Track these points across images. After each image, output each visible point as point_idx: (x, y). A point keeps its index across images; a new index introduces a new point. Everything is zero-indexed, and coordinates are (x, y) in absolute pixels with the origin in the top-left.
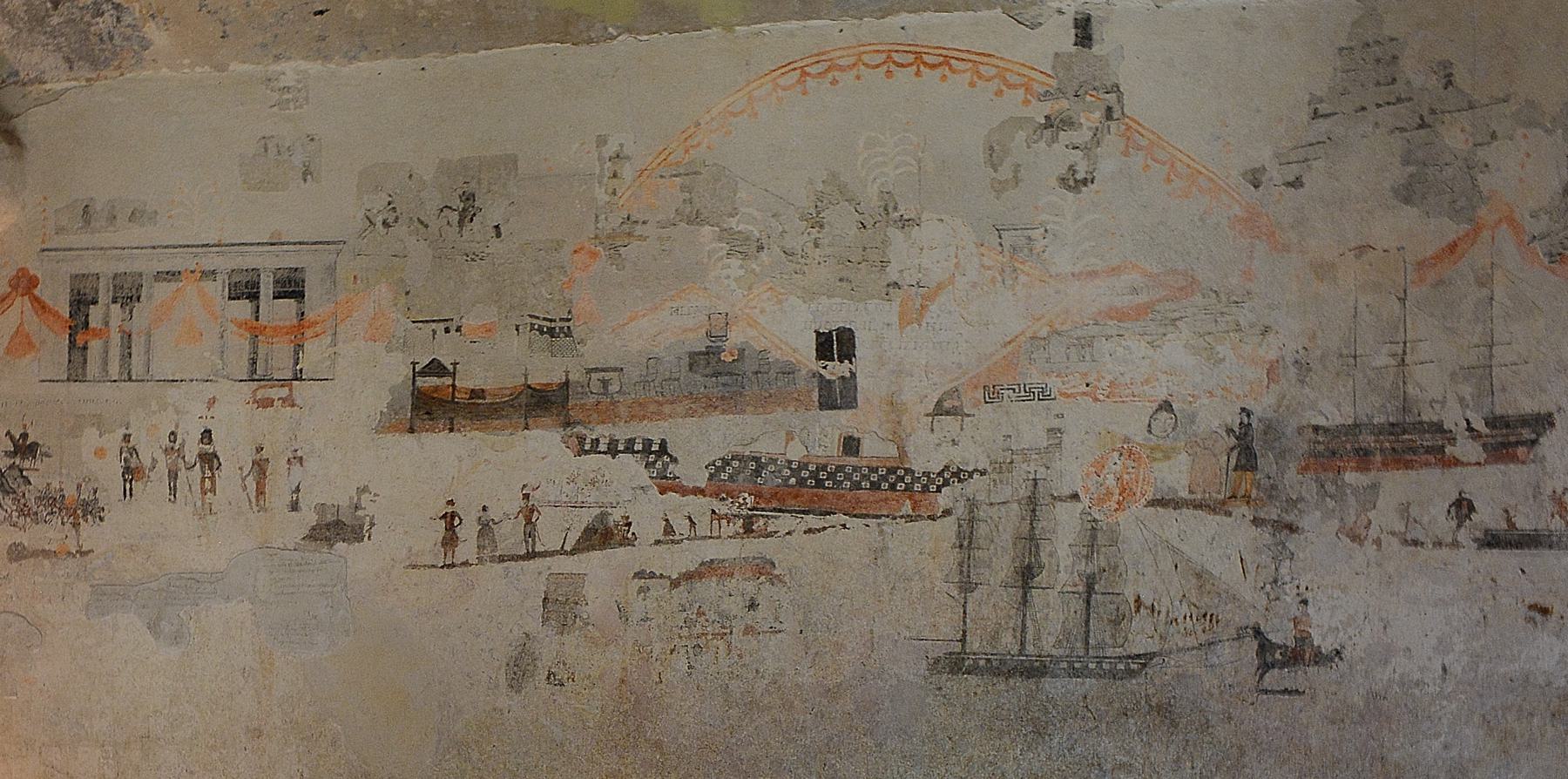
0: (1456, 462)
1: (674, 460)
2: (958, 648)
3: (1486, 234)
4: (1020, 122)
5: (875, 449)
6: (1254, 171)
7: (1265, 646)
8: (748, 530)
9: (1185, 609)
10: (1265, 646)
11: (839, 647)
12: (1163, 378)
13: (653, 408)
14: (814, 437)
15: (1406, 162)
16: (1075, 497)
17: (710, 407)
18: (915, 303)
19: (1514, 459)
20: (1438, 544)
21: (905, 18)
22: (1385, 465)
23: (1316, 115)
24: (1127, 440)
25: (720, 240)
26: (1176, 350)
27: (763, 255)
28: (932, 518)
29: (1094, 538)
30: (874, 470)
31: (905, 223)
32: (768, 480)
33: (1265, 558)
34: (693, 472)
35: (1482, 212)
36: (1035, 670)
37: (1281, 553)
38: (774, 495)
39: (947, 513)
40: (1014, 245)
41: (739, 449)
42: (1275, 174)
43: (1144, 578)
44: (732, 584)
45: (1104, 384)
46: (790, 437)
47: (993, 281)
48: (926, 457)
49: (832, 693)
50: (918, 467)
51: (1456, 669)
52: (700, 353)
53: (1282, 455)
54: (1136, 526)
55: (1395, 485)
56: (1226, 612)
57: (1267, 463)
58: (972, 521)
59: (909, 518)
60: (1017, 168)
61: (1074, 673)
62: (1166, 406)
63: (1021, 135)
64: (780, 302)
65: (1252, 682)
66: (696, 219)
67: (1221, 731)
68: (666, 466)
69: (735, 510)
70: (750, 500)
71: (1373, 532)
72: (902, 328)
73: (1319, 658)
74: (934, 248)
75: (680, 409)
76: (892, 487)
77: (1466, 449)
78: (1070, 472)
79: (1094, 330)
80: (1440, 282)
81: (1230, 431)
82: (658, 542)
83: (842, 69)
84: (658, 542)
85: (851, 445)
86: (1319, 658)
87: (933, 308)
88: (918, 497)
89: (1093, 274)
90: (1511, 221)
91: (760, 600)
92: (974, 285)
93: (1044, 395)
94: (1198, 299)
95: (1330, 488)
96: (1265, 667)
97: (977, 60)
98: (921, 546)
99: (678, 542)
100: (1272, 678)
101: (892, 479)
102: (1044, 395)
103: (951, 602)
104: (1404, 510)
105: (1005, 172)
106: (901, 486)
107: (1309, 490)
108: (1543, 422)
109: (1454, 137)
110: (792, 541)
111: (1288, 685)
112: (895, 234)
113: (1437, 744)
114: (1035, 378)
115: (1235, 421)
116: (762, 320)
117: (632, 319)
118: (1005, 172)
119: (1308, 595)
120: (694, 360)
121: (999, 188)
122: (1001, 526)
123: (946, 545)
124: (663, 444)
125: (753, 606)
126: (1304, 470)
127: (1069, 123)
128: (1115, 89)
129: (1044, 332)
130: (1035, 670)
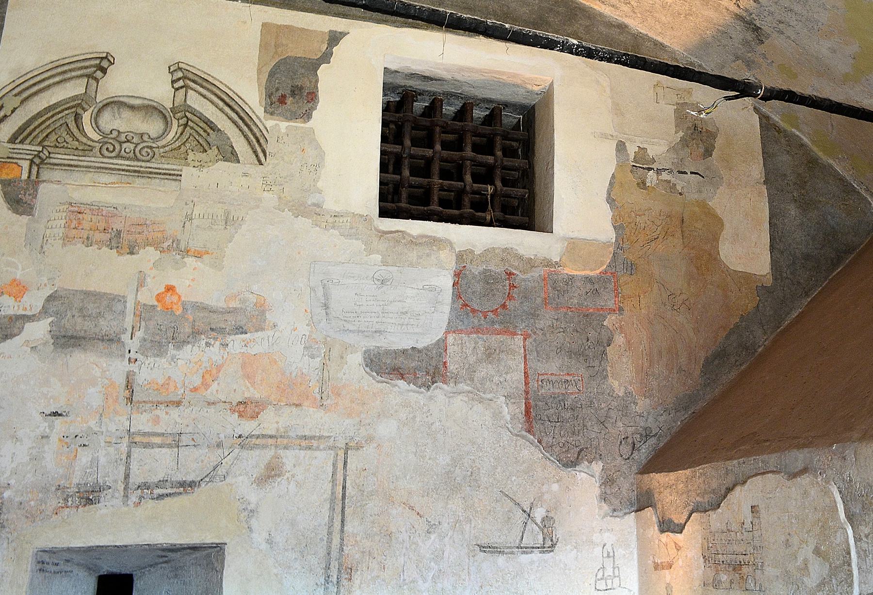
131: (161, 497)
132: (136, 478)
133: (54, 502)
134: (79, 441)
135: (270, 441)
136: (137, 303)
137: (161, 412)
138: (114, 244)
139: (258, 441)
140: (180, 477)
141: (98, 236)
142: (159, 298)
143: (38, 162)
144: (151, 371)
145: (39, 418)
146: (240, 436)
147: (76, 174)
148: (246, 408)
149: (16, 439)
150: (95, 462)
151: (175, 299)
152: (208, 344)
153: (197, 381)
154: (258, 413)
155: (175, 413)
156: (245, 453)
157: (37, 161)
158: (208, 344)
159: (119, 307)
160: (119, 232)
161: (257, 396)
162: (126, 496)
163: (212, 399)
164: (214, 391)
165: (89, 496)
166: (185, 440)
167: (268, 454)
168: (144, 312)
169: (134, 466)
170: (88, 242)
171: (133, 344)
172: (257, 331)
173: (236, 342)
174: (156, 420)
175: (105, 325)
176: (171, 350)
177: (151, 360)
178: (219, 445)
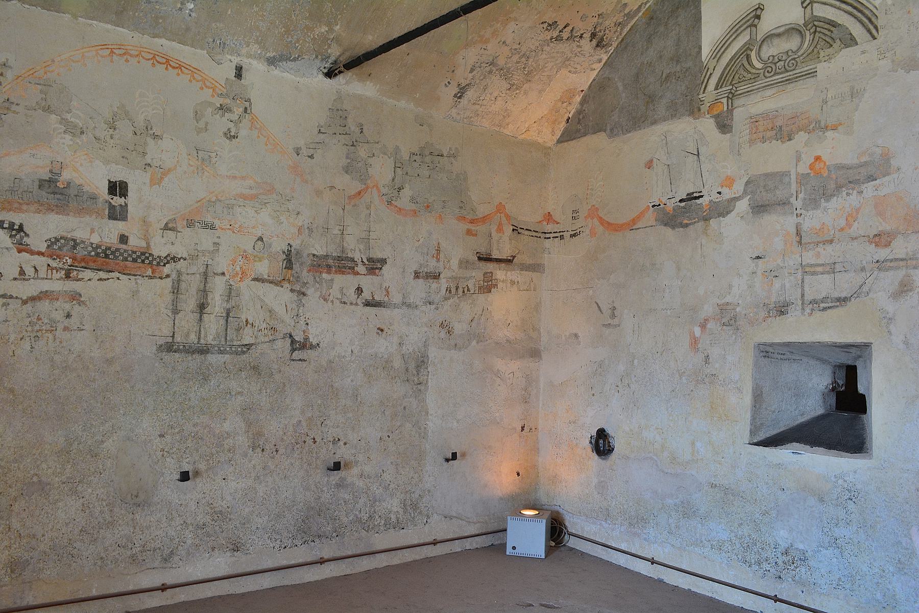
0: (358, 274)
1: (27, 235)
2: (170, 340)
3: (369, 190)
4: (210, 104)
5: (135, 242)
6: (298, 148)
7: (293, 342)
8: (68, 276)
9: (264, 325)
10: (293, 342)
11: (114, 338)
12: (260, 227)
13: (16, 205)
14: (106, 233)
15: (347, 158)
16: (223, 274)
17: (50, 209)
18: (159, 175)
19: (375, 274)
20: (351, 304)
21: (163, 41)
22: (336, 272)
23: (320, 132)
24: (245, 251)
25: (61, 123)
26: (265, 216)
27: (84, 137)
28: (161, 278)
29: (230, 293)
30: (134, 252)
31: (155, 137)
32: (80, 252)
33: (294, 306)
34: (38, 242)
35: (369, 182)
36: (204, 351)
37: (300, 304)
38: (83, 260)
39: (168, 276)
40: (203, 158)
41: (65, 234)
42: (305, 152)
43: (249, 312)
44: (57, 304)
45: (237, 226)
46: (92, 231)
47: (193, 172)
48: (160, 249)
49: (109, 362)
50: (156, 253)
51: (355, 351)
52: (46, 180)
53: (301, 264)
54: (247, 289)
55: (340, 280)
56: (280, 327)
57: (296, 267)
58: (179, 281)
59: (151, 278)
60: (207, 124)
61: (221, 352)
62: (261, 239)
63: (210, 110)
64: (91, 162)
65: (288, 357)
66: (48, 109)
67: (277, 377)
68: (22, 238)
69: (61, 265)
70: (70, 261)
71: (331, 298)
72: (151, 186)
73: (312, 347)
74: (167, 151)
75: (32, 208)
76: (144, 261)
77: (361, 269)
78: (222, 263)
79: (235, 202)
80: (354, 205)
81: (284, 252)
82: (15, 279)
83: (131, 55)
84: (15, 279)
85: (123, 239)
86: (312, 347)
87: (166, 179)
88: (154, 267)
89: (235, 177)
90: (377, 187)
91: (72, 313)
92: (185, 172)
93: (212, 228)
94: (274, 195)
95: (318, 280)
96: (293, 350)
97: (193, 71)
98: (154, 291)
99: (27, 280)
100: (297, 355)
101: (143, 257)
102: (212, 228)
103: (167, 318)
104: (342, 289)
105: (201, 124)
106: (147, 261)
107: (310, 280)
108: (383, 261)
109: (362, 152)
110: (90, 284)
111: (301, 357)
112: (150, 141)
113: (349, 380)
114: (209, 219)
115: (286, 248)
116: (81, 169)
117: (7, 155)
118: (201, 124)
119: (309, 321)
120: (42, 184)
121: (199, 131)
122: (192, 285)
123: (167, 292)
124: (21, 226)
125: (68, 316)
126: (309, 271)
127: (229, 110)
128: (249, 100)
129: (214, 199)
130: (204, 351)
131: (825, 309)
132: (808, 297)
133: (763, 314)
134: (773, 274)
135: (902, 263)
136: (798, 174)
137: (820, 249)
138: (779, 136)
139: (892, 264)
140: (836, 295)
141: (769, 134)
142: (811, 167)
143: (731, 96)
144: (812, 221)
145: (749, 259)
146: (877, 262)
147: (752, 96)
148: (880, 239)
149: (739, 275)
150: (783, 286)
151: (822, 165)
152: (848, 194)
153: (843, 223)
154: (890, 242)
155: (829, 248)
156: (882, 274)
157: (730, 96)
158: (848, 194)
159: (786, 179)
160: (781, 127)
161: (888, 228)
162: (803, 309)
163: (854, 235)
164: (857, 228)
165: (782, 310)
166: (838, 267)
167: (901, 274)
168: (803, 179)
169: (807, 289)
170: (763, 140)
171: (798, 204)
172: (884, 176)
173: (869, 189)
174: (818, 255)
175: (780, 194)
176: (823, 204)
177: (811, 213)
178: (863, 269)
